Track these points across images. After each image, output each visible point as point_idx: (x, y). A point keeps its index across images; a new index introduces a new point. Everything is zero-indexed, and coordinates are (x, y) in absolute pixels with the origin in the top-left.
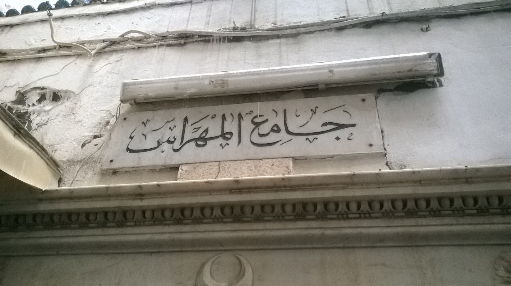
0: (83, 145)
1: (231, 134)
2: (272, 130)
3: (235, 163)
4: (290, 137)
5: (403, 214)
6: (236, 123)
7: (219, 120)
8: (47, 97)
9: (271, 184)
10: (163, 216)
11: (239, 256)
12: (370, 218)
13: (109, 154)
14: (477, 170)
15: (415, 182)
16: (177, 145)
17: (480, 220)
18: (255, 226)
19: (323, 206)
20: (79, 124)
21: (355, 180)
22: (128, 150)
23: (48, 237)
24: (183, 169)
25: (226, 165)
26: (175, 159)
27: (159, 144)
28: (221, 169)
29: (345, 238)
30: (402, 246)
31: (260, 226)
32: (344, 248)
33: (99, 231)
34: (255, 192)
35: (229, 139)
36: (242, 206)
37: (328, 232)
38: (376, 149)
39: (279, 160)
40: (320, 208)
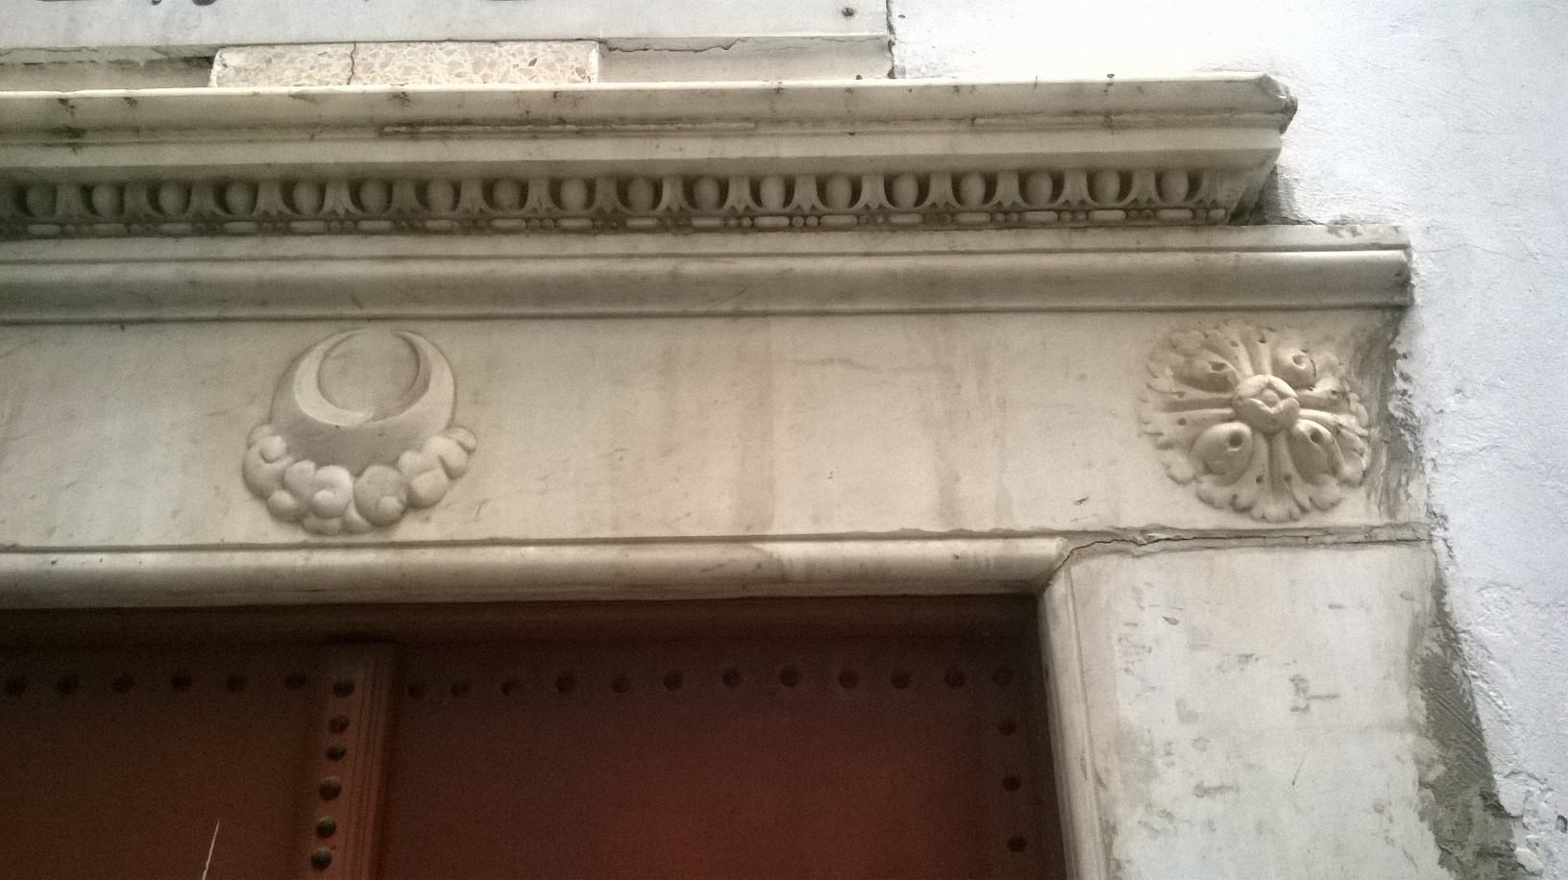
3: (406, 49)
5: (916, 219)
9: (515, 112)
10: (158, 208)
11: (409, 335)
12: (821, 228)
14: (1139, 88)
15: (957, 120)
17: (1127, 238)
18: (466, 246)
19: (679, 189)
21: (782, 107)
24: (228, 62)
25: (374, 56)
28: (359, 70)
29: (742, 286)
30: (901, 313)
32: (736, 315)
34: (465, 137)
37: (693, 268)
38: (864, 27)
39: (556, 46)
40: (670, 195)
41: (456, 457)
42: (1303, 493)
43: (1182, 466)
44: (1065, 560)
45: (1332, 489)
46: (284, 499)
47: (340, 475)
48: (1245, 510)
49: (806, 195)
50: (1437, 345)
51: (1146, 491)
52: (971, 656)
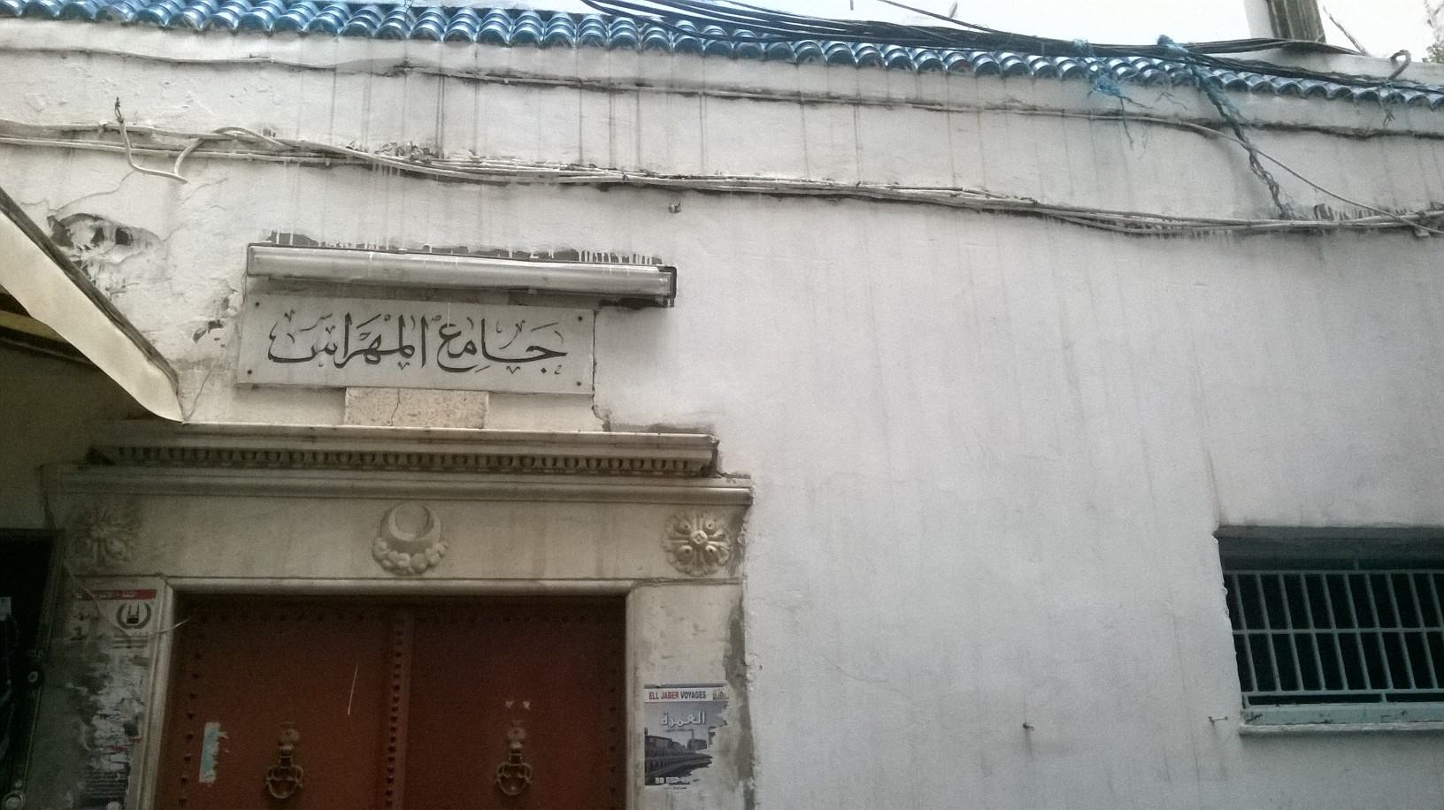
0: (197, 337)
1: (412, 348)
2: (466, 349)
4: (487, 362)
6: (418, 332)
7: (395, 323)
8: (107, 233)
13: (246, 361)
16: (339, 358)
17: (663, 481)
20: (181, 299)
22: (271, 357)
23: (193, 477)
26: (340, 378)
27: (314, 353)
31: (450, 477)
33: (258, 473)
35: (409, 356)
36: (432, 456)
37: (521, 487)
40: (515, 463)
41: (442, 549)
42: (706, 568)
43: (672, 557)
44: (633, 588)
45: (716, 567)
46: (388, 563)
47: (406, 556)
48: (688, 573)
49: (560, 464)
50: (756, 519)
51: (660, 566)
52: (600, 618)
